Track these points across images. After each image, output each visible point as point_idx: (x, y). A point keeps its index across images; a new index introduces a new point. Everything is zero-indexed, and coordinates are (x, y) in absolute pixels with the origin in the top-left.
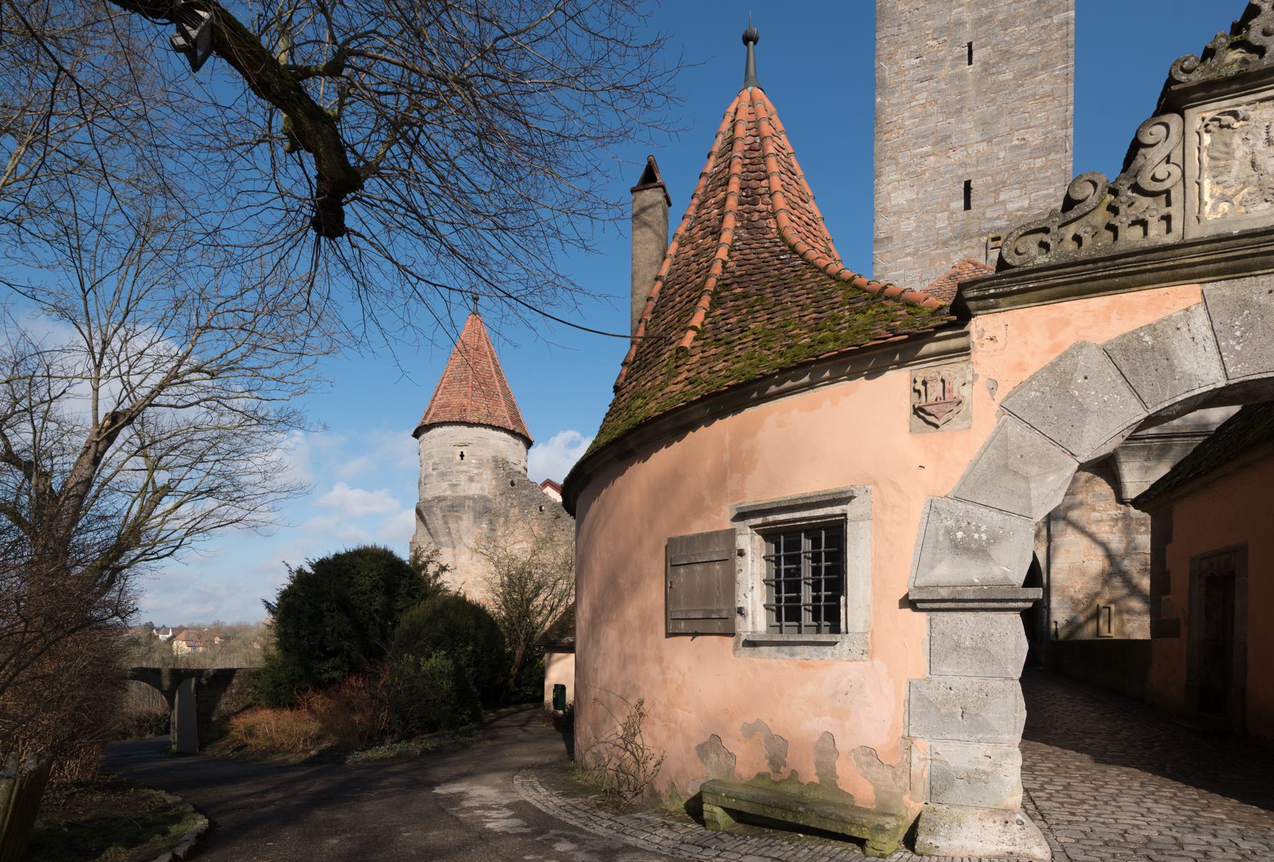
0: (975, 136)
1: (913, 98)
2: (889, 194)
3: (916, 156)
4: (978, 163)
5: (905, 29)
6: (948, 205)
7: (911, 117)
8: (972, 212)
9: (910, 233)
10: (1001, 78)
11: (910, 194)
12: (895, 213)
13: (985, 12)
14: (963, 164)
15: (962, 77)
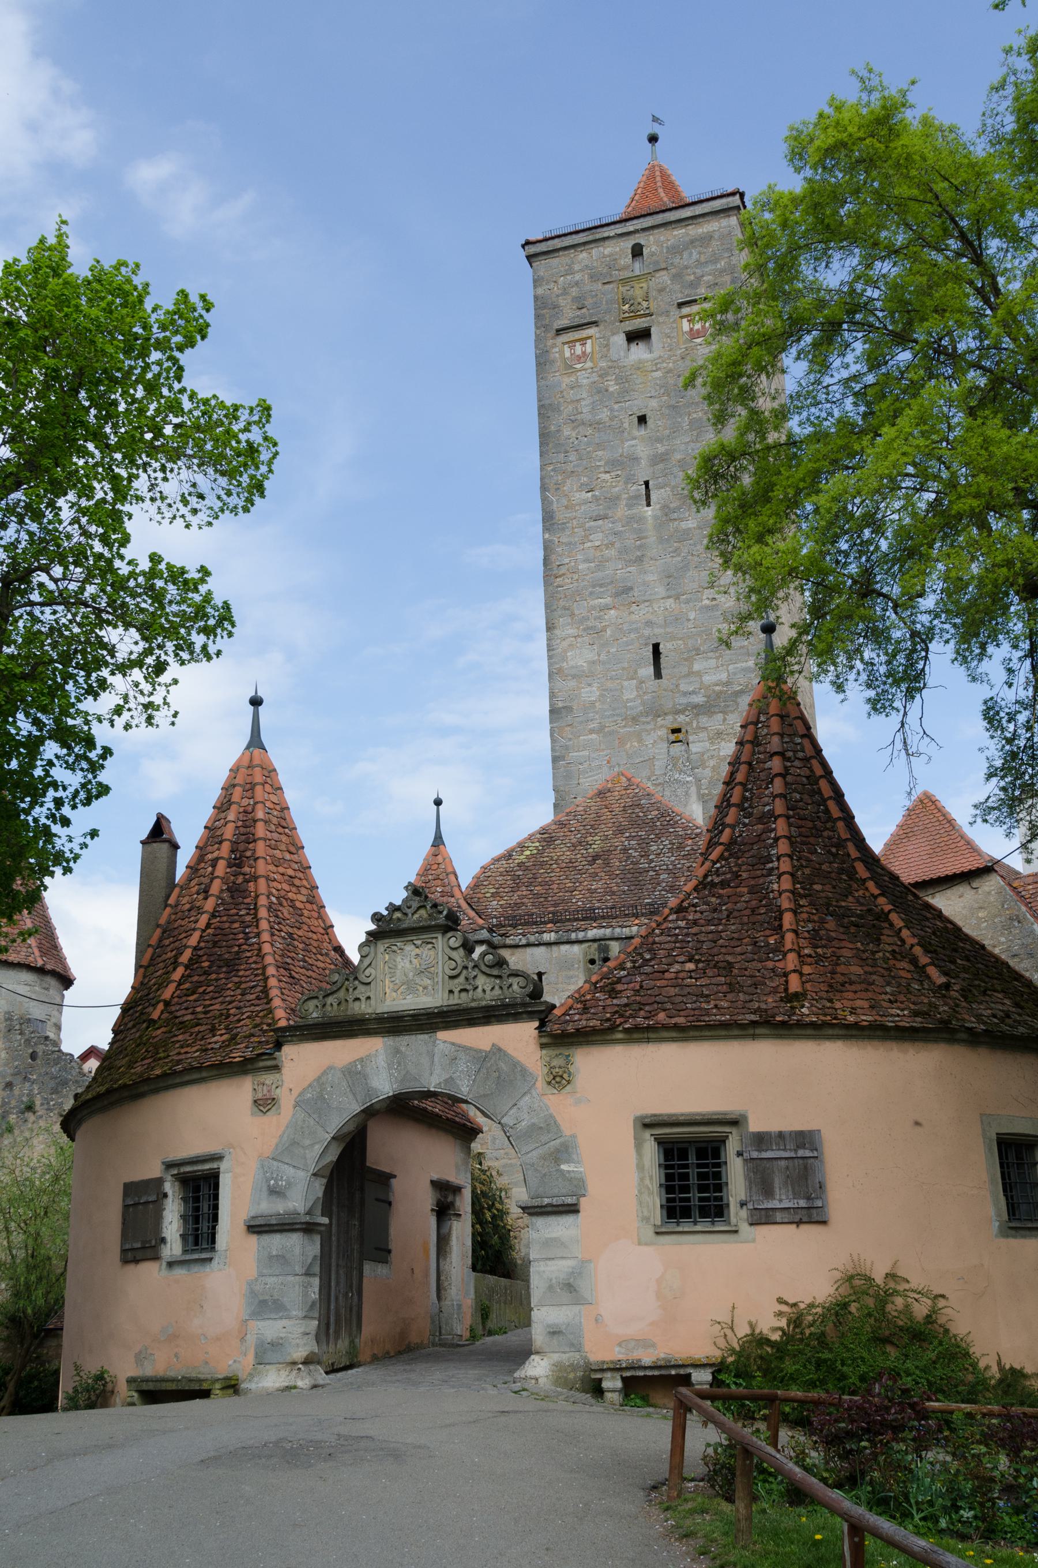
0: (661, 590)
1: (586, 538)
2: (565, 651)
3: (594, 608)
4: (666, 624)
5: (573, 457)
6: (636, 672)
7: (587, 561)
8: (664, 681)
9: (593, 703)
10: (684, 525)
11: (589, 655)
12: (574, 677)
13: (661, 449)
14: (649, 623)
15: (641, 520)
